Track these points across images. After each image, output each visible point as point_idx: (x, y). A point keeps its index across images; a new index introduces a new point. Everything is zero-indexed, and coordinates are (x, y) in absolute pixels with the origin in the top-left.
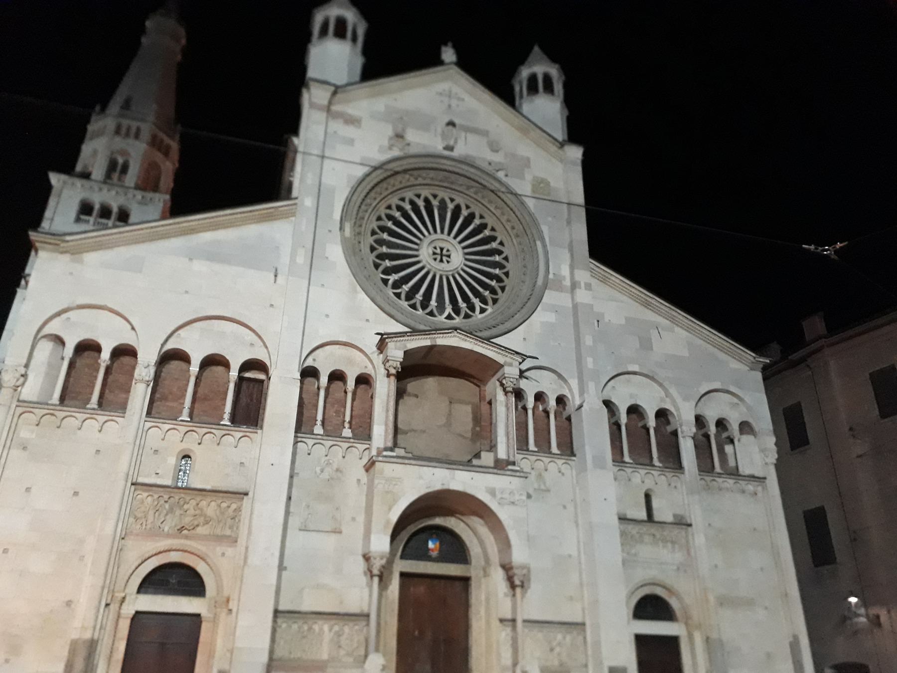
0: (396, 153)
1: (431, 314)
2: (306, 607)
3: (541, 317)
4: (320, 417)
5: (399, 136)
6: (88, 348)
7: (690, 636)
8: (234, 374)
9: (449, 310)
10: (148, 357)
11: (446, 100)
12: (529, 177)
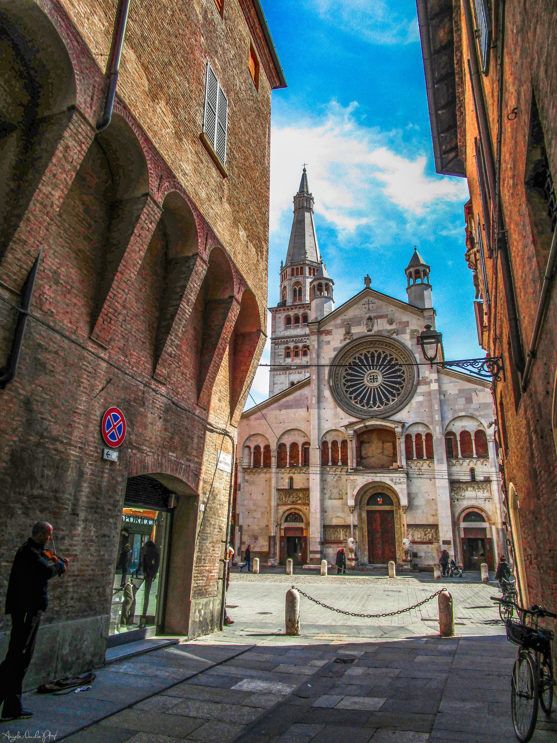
0: (348, 341)
1: (371, 407)
2: (334, 524)
3: (417, 399)
4: (330, 459)
5: (348, 333)
6: (257, 448)
7: (491, 528)
8: (300, 449)
9: (378, 404)
10: (274, 447)
11: (367, 306)
12: (408, 331)
